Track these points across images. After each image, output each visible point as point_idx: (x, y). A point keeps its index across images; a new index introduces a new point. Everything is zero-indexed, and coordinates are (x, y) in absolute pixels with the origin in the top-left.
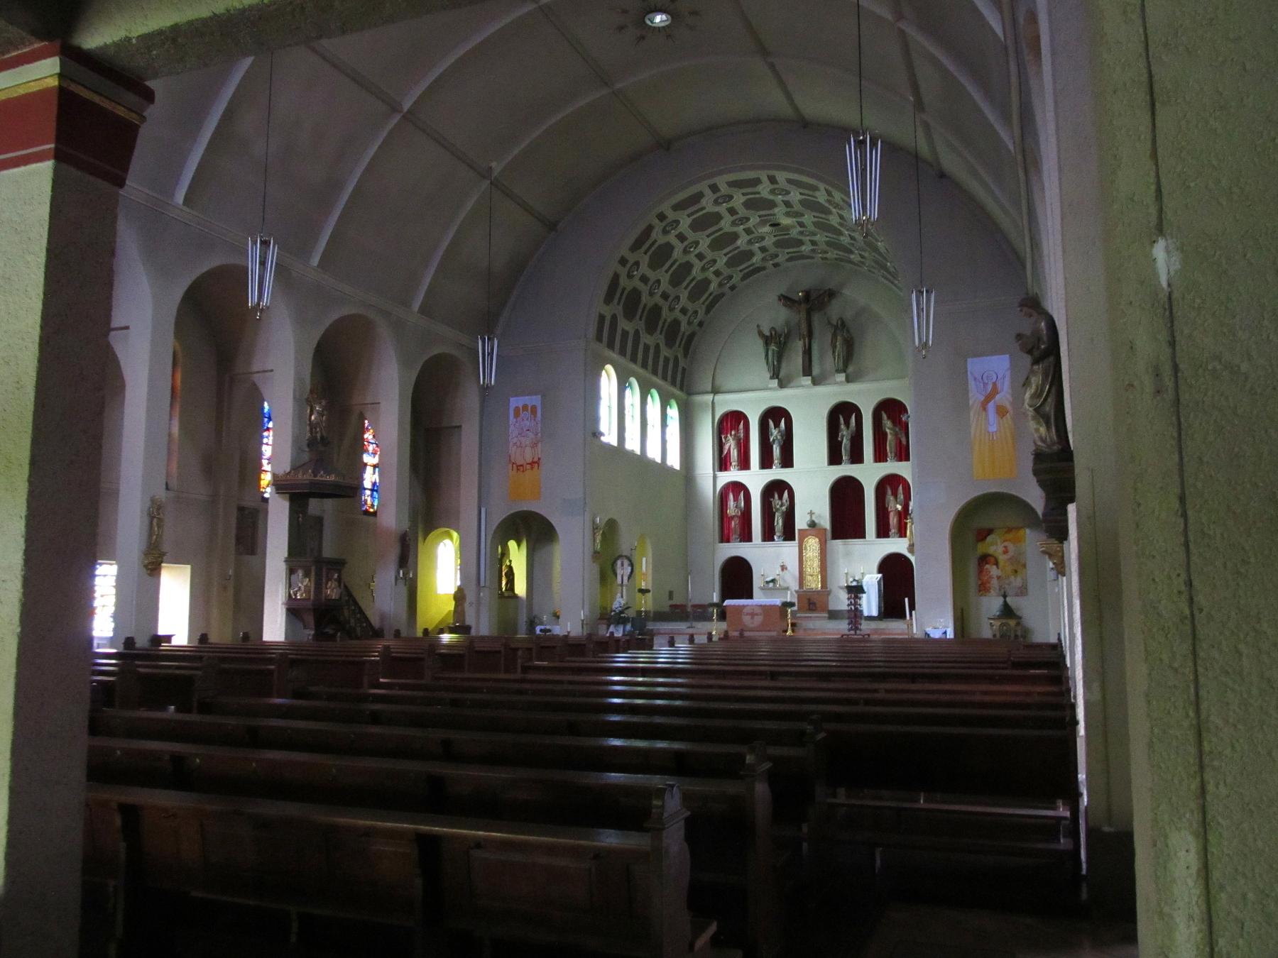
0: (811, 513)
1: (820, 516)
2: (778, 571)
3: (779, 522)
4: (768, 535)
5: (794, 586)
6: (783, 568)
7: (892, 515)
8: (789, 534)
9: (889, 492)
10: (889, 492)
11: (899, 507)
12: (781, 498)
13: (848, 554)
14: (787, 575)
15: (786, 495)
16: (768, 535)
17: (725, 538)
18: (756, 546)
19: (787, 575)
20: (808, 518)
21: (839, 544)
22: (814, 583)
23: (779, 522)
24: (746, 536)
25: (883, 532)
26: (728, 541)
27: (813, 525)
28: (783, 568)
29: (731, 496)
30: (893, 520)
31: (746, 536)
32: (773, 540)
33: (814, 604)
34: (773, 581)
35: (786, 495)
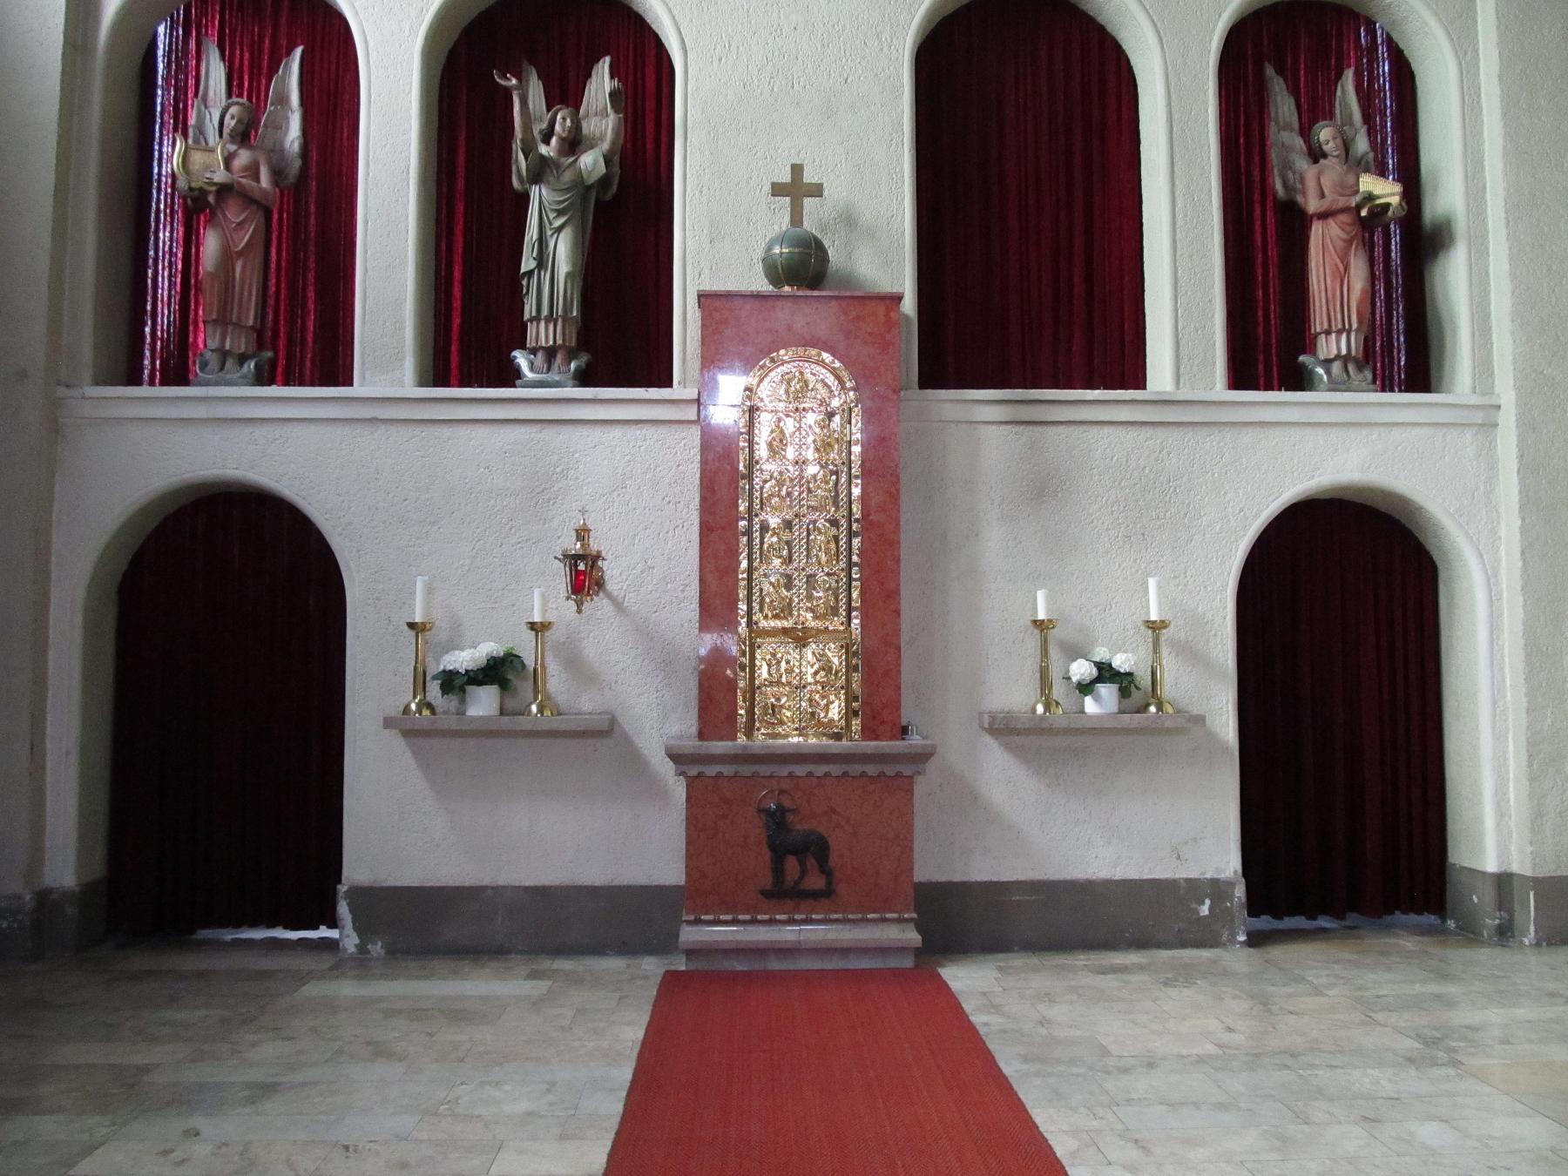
0: (796, 189)
1: (848, 220)
2: (546, 595)
3: (553, 253)
4: (471, 338)
5: (659, 719)
6: (584, 576)
7: (1324, 240)
8: (624, 338)
9: (1283, 106)
10: (1283, 106)
11: (1387, 191)
12: (566, 93)
13: (1043, 490)
14: (600, 632)
15: (601, 83)
16: (471, 338)
17: (149, 349)
18: (380, 415)
19: (600, 632)
20: (774, 221)
21: (980, 407)
22: (802, 688)
23: (553, 253)
24: (307, 338)
25: (1267, 347)
26: (177, 372)
27: (804, 267)
28: (584, 576)
29: (215, 73)
30: (1337, 280)
31: (307, 338)
32: (509, 376)
33: (816, 849)
34: (498, 671)
35: (601, 83)
